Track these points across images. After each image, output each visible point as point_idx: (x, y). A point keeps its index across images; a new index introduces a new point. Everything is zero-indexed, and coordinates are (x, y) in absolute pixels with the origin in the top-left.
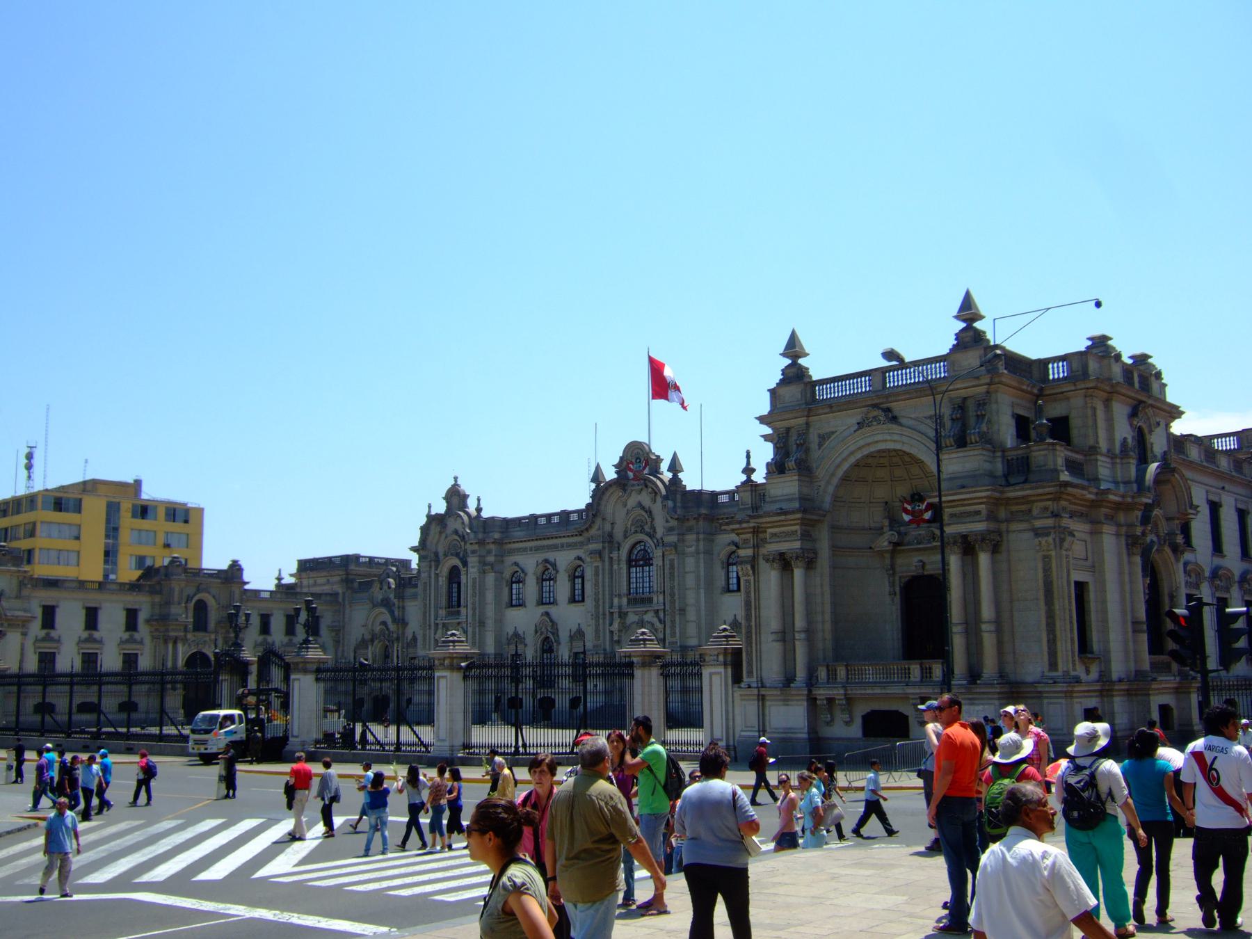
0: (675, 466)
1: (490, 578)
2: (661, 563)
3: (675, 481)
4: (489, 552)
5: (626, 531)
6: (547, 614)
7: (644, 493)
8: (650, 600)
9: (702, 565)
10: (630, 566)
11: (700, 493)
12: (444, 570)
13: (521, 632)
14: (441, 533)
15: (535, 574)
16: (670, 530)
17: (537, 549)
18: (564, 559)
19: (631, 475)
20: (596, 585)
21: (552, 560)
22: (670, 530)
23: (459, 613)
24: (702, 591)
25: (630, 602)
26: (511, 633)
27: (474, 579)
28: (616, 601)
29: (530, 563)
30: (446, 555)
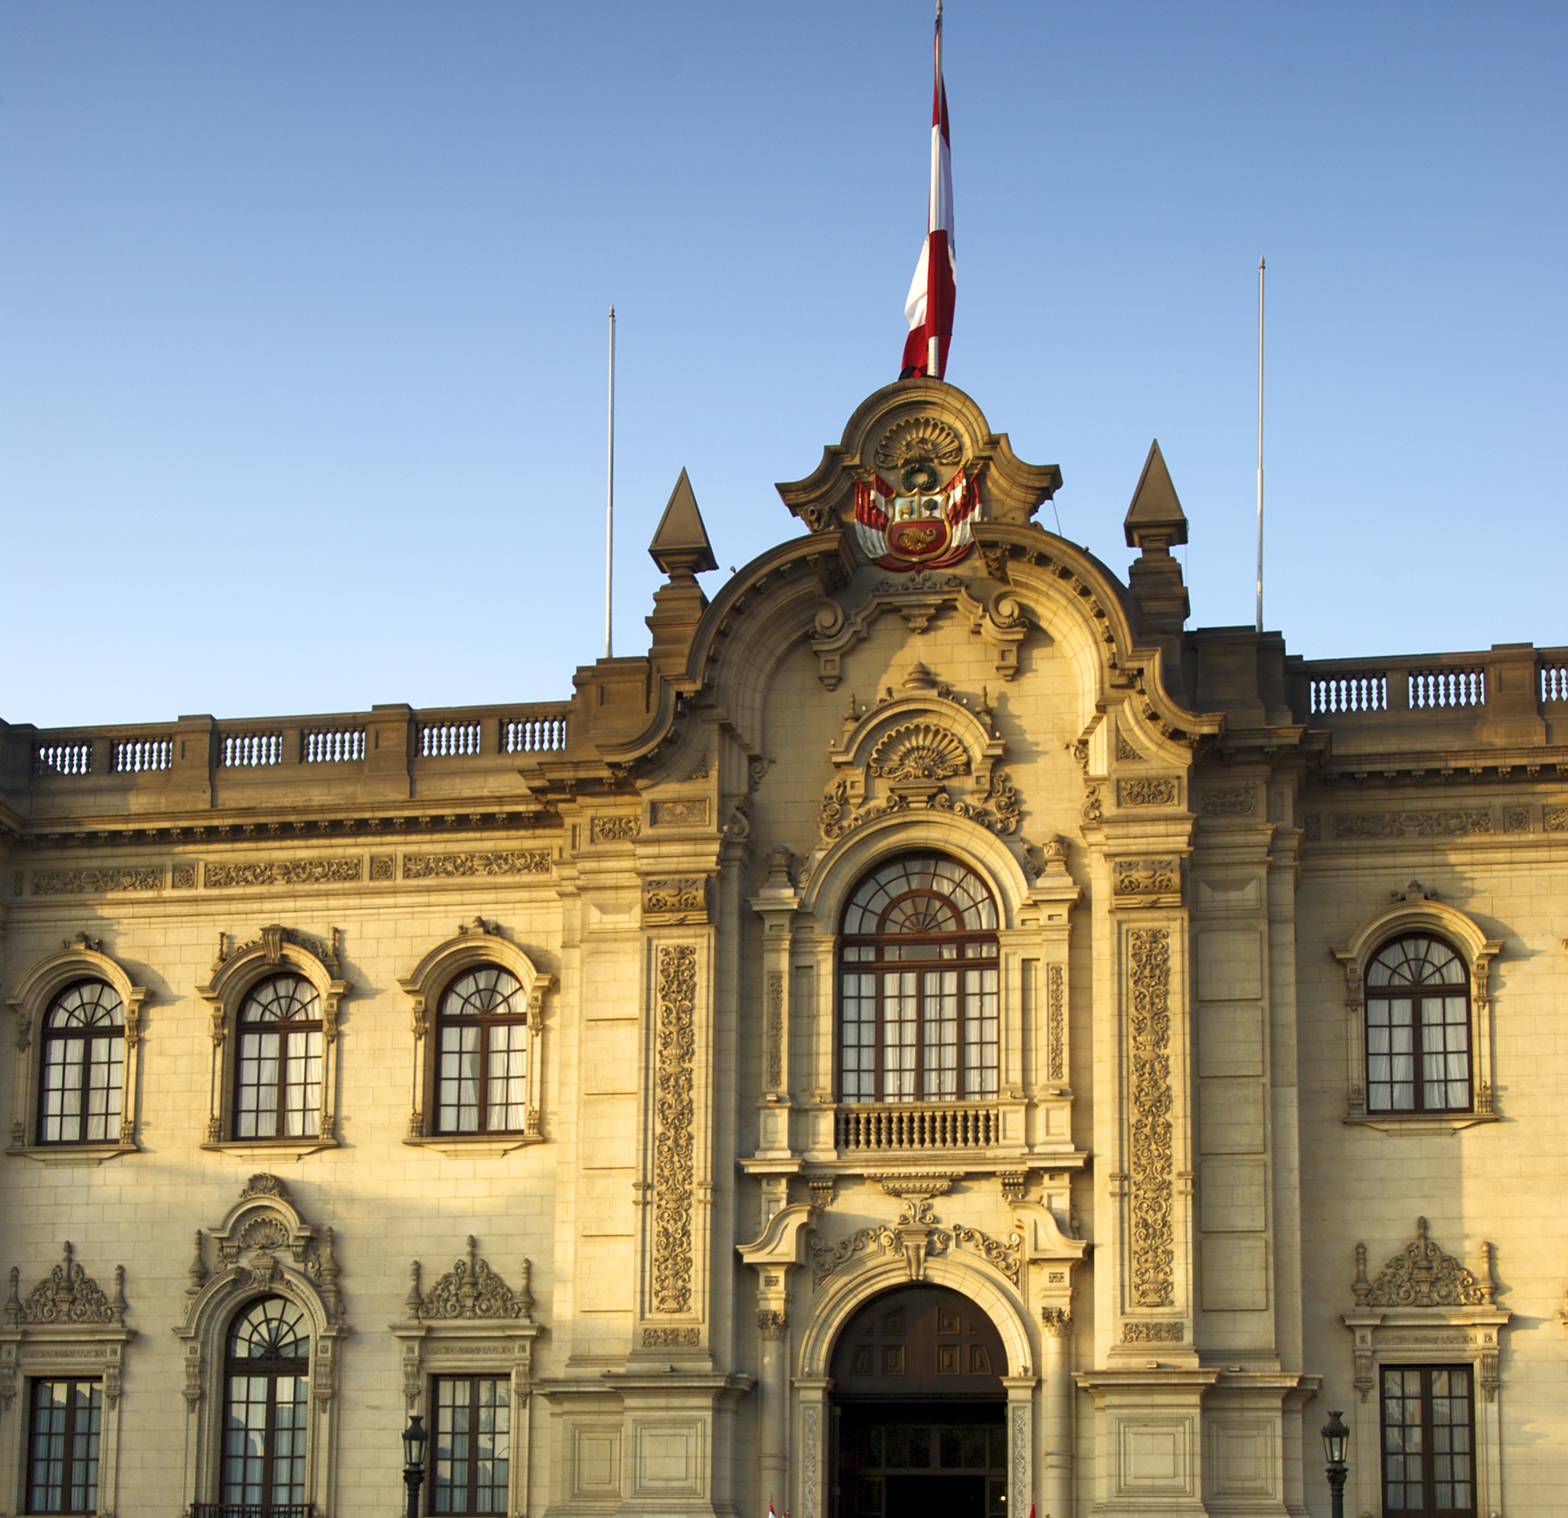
6: (282, 1188)
7: (952, 632)
8: (982, 1128)
9: (1288, 974)
10: (842, 968)
13: (100, 1270)
18: (391, 933)
19: (875, 542)
24: (1291, 1094)
26: (37, 1270)
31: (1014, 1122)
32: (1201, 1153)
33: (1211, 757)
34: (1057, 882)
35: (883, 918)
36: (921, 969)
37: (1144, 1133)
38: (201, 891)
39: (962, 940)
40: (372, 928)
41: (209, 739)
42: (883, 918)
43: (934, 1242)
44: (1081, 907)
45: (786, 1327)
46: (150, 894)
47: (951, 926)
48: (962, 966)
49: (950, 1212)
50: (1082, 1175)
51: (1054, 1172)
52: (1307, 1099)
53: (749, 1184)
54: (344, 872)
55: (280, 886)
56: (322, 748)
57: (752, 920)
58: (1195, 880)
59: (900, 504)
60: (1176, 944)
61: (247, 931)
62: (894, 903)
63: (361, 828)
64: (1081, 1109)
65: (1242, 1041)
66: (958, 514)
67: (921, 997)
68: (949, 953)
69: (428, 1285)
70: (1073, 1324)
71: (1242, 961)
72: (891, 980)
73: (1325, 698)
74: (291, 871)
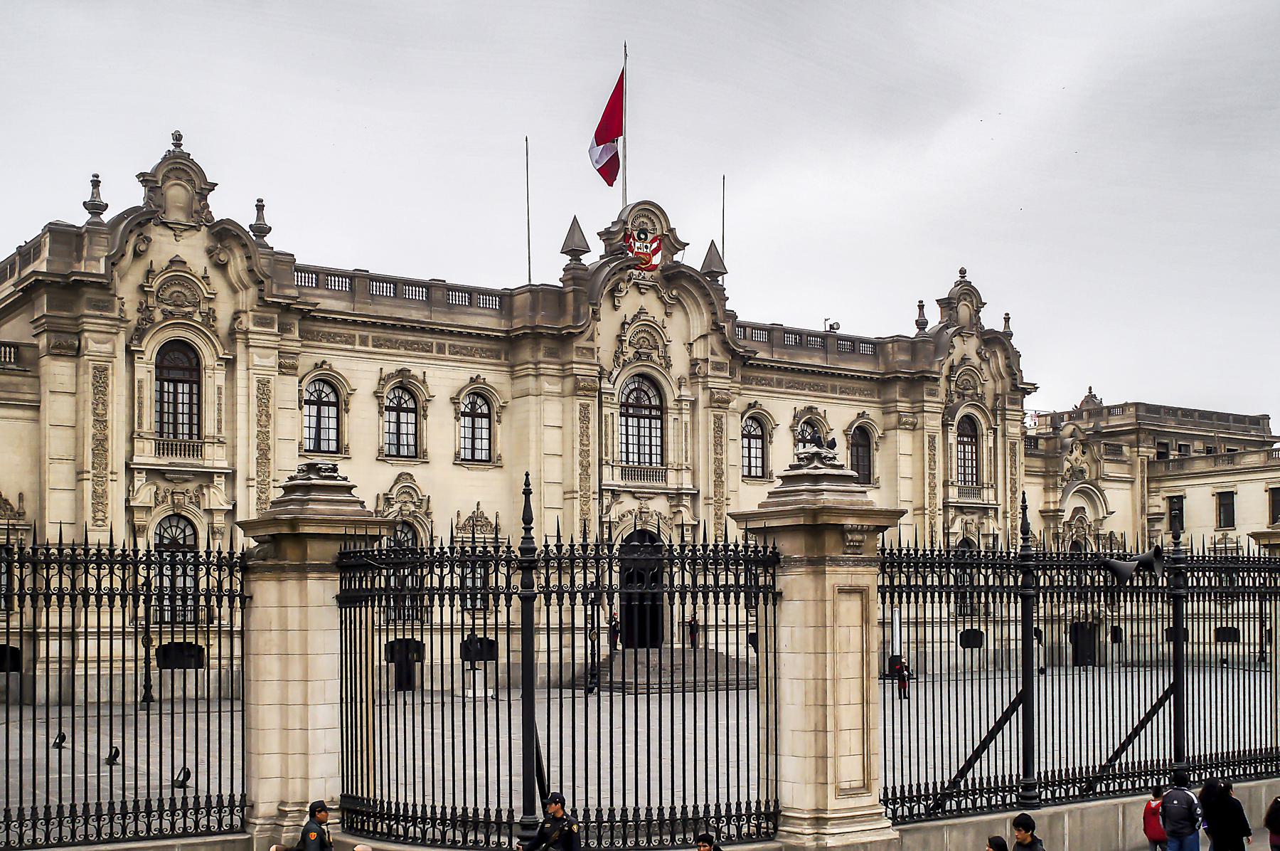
0: (715, 265)
1: (286, 390)
2: (686, 418)
4: (284, 329)
12: (151, 347)
14: (137, 255)
15: (377, 395)
16: (718, 367)
20: (584, 434)
21: (416, 371)
22: (718, 367)
23: (196, 450)
25: (625, 473)
27: (263, 385)
28: (606, 470)
29: (362, 372)
30: (144, 309)
31: (671, 475)
34: (685, 392)
35: (628, 397)
36: (639, 417)
38: (370, 349)
39: (651, 408)
40: (438, 373)
41: (359, 281)
42: (628, 397)
44: (694, 404)
46: (349, 347)
47: (647, 403)
48: (650, 418)
50: (695, 497)
51: (687, 494)
55: (402, 351)
56: (410, 292)
59: (638, 244)
61: (390, 368)
62: (631, 391)
63: (432, 331)
66: (655, 252)
67: (639, 427)
68: (647, 413)
69: (463, 520)
72: (630, 419)
74: (408, 345)
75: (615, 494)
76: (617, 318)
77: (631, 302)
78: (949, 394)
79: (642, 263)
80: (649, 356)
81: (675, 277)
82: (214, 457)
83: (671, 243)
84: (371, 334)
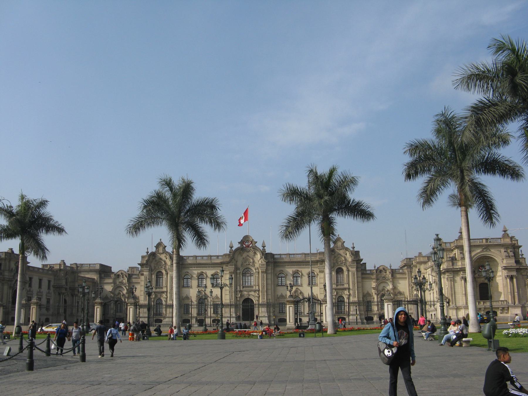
3: (264, 250)
5: (242, 264)
8: (252, 287)
11: (271, 254)
16: (264, 265)
17: (197, 267)
18: (210, 272)
23: (162, 288)
28: (238, 287)
30: (155, 267)
32: (267, 289)
33: (267, 263)
34: (257, 270)
37: (263, 288)
43: (249, 295)
45: (239, 301)
49: (250, 293)
50: (259, 291)
52: (274, 285)
53: (236, 291)
54: (206, 267)
57: (236, 273)
58: (266, 272)
60: (265, 275)
61: (199, 272)
64: (259, 286)
65: (269, 282)
70: (258, 301)
71: (269, 276)
73: (275, 256)
74: (202, 267)
75: (241, 291)
76: (242, 258)
77: (245, 255)
78: (334, 263)
79: (248, 246)
80: (249, 264)
81: (255, 248)
82: (164, 289)
83: (253, 242)
84: (195, 266)
